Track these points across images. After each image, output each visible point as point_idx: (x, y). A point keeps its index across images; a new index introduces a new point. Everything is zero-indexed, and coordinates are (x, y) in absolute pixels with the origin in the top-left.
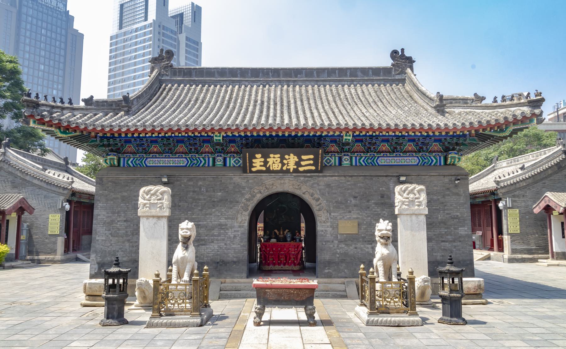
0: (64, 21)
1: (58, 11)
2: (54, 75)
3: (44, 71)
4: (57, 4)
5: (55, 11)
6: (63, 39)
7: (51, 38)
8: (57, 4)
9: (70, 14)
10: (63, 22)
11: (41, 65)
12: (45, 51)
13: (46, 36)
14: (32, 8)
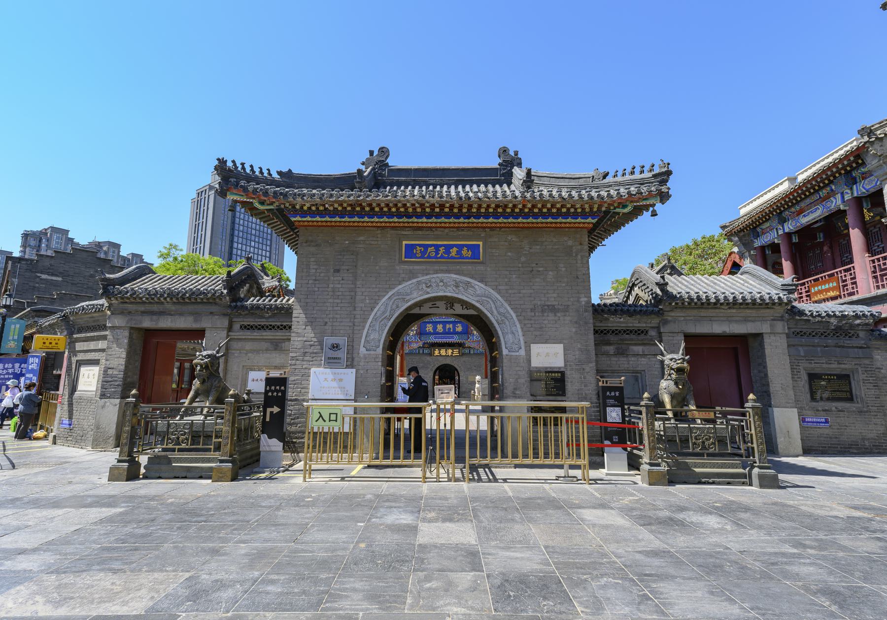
2: (262, 250)
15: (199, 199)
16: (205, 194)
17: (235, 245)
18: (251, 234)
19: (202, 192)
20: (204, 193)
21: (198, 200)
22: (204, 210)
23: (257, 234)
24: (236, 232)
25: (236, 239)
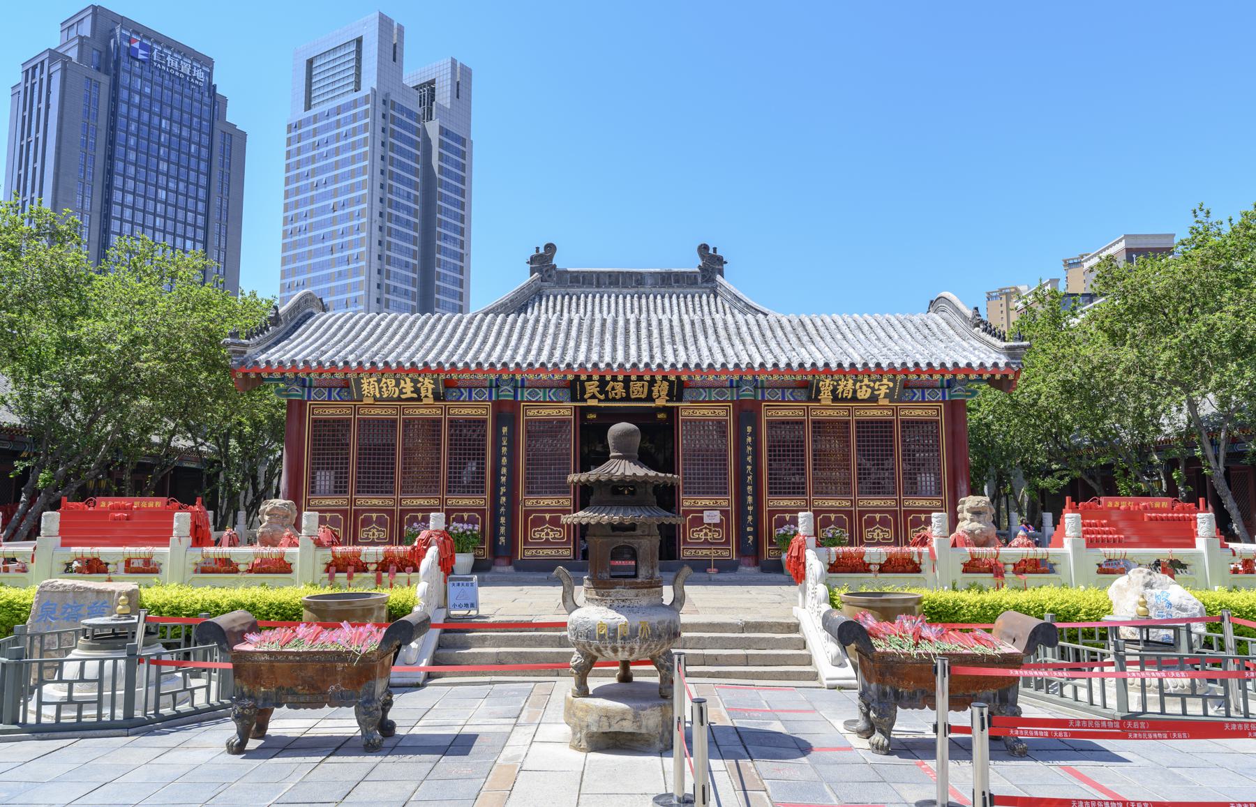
0: (205, 105)
1: (194, 84)
2: (186, 210)
3: (166, 203)
4: (191, 72)
5: (187, 85)
6: (205, 140)
7: (180, 136)
8: (191, 72)
9: (218, 91)
10: (205, 108)
11: (160, 191)
12: (168, 161)
13: (170, 133)
14: (141, 77)
15: (29, 85)
16: (42, 72)
17: (117, 196)
18: (158, 172)
19: (34, 68)
20: (38, 71)
21: (26, 88)
22: (39, 110)
24: (119, 166)
25: (118, 181)
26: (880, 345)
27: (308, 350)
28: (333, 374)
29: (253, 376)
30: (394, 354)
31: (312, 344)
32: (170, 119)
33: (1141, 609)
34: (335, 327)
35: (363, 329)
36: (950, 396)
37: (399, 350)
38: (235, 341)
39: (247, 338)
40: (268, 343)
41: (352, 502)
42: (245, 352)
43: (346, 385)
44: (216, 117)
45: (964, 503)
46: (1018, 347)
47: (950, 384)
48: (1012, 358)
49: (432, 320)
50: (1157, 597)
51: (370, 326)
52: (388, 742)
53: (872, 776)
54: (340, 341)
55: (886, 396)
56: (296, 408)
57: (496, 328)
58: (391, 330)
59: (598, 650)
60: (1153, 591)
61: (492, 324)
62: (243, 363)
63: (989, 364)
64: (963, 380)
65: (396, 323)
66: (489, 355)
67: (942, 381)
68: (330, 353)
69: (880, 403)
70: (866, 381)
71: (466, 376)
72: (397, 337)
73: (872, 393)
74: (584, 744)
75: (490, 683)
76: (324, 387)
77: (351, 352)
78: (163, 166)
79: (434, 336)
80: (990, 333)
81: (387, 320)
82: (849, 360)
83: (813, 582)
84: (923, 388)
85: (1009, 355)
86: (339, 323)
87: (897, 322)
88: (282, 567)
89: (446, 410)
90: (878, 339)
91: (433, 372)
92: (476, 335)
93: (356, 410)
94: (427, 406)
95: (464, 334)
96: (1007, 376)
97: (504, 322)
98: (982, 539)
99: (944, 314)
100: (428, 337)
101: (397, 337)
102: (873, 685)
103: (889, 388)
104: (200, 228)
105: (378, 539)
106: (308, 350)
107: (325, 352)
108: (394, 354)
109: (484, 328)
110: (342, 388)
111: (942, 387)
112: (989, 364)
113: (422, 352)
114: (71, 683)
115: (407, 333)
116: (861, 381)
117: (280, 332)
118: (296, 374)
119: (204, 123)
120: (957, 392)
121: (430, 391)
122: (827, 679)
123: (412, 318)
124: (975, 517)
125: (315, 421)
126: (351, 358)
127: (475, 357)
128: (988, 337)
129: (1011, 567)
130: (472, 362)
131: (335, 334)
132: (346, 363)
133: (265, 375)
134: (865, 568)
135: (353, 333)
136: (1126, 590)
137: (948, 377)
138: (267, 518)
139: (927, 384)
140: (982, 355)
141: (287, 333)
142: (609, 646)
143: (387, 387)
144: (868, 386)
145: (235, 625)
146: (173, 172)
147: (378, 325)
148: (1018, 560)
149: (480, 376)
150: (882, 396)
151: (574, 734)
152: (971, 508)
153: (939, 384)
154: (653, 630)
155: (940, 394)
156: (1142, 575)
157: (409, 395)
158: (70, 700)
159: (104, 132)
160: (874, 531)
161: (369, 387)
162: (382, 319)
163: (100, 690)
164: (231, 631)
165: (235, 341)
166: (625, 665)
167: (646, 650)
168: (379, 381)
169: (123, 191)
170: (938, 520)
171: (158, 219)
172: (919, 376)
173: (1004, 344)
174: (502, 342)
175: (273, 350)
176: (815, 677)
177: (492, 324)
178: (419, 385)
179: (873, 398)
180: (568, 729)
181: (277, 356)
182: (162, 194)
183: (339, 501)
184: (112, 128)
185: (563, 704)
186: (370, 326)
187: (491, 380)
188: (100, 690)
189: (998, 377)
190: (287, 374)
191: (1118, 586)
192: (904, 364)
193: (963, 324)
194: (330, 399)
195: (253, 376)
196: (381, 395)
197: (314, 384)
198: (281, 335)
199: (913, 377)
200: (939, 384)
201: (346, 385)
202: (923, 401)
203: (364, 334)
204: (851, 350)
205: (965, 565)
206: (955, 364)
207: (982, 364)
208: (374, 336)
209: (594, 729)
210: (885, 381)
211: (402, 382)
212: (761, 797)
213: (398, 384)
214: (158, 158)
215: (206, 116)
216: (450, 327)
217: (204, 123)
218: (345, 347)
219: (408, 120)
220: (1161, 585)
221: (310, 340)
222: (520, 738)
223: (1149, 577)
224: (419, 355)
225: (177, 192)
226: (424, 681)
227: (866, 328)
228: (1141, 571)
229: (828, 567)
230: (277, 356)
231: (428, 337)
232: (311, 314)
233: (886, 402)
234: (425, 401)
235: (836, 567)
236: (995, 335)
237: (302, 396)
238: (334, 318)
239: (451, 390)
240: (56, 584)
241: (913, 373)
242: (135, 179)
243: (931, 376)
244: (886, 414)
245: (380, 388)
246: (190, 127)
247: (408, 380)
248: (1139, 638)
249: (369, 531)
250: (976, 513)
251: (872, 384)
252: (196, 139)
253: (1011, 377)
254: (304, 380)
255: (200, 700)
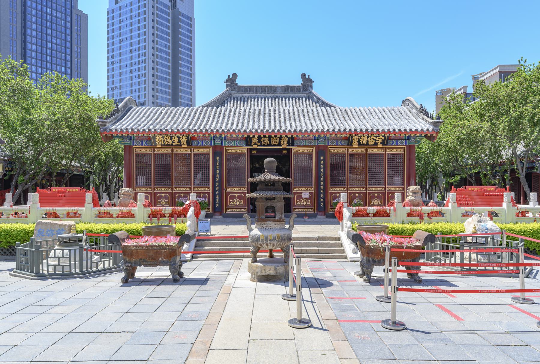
2: (61, 52)
3: (51, 49)
6: (68, 18)
7: (56, 17)
11: (48, 43)
12: (52, 29)
13: (51, 15)
17: (29, 46)
18: (47, 34)
23: (54, 34)
24: (29, 31)
25: (28, 39)
26: (379, 121)
27: (132, 124)
28: (144, 135)
29: (110, 135)
30: (170, 126)
31: (133, 121)
32: (51, 8)
33: (474, 230)
34: (143, 113)
35: (155, 114)
36: (409, 143)
37: (171, 124)
38: (101, 120)
39: (106, 119)
40: (115, 121)
41: (153, 189)
42: (106, 125)
43: (149, 139)
44: (73, 7)
45: (410, 188)
46: (438, 122)
47: (409, 138)
48: (435, 127)
49: (185, 110)
50: (482, 226)
51: (158, 113)
52: (181, 279)
53: (362, 289)
54: (145, 120)
55: (381, 143)
56: (128, 149)
57: (213, 114)
58: (167, 115)
59: (261, 245)
60: (481, 223)
61: (211, 112)
62: (105, 130)
63: (425, 129)
64: (414, 136)
65: (169, 112)
66: (211, 126)
67: (405, 136)
68: (142, 125)
69: (378, 146)
70: (373, 137)
71: (201, 135)
72: (170, 118)
73: (375, 142)
74: (256, 279)
75: (217, 260)
76: (140, 140)
77: (151, 125)
78: (49, 31)
79: (186, 118)
80: (426, 116)
81: (165, 110)
82: (365, 128)
83: (346, 221)
84: (397, 140)
85: (434, 125)
86: (144, 111)
87: (387, 111)
88: (131, 215)
89: (192, 150)
90: (379, 118)
91: (187, 134)
92: (204, 117)
93: (154, 150)
94: (184, 148)
95: (199, 116)
96: (433, 134)
97: (216, 111)
98: (416, 203)
99: (408, 107)
100: (183, 118)
101: (170, 118)
102: (365, 258)
103: (382, 140)
104: (68, 61)
105: (165, 204)
106: (132, 124)
107: (140, 125)
108: (170, 126)
109: (208, 114)
110: (147, 140)
111: (405, 139)
112: (425, 129)
113: (182, 125)
114: (59, 258)
115: (174, 116)
116: (371, 137)
117: (119, 116)
118: (128, 135)
119: (67, 10)
120: (412, 142)
121: (185, 142)
122: (350, 258)
123: (176, 109)
124: (414, 195)
125: (136, 154)
126: (151, 127)
127: (205, 127)
128: (426, 118)
129: (427, 215)
130: (203, 129)
131: (143, 117)
132: (149, 130)
133: (114, 135)
134: (368, 215)
135: (151, 116)
136: (471, 223)
137: (407, 135)
138: (122, 196)
139: (399, 138)
140: (423, 126)
141: (122, 116)
142: (265, 243)
143: (167, 140)
144: (373, 139)
145: (122, 236)
146: (54, 34)
147: (161, 112)
148: (429, 212)
149: (207, 135)
150: (379, 143)
151: (252, 276)
152: (412, 191)
153: (404, 138)
154: (282, 237)
155: (404, 142)
156: (477, 217)
157: (176, 143)
158: (59, 265)
159: (20, 15)
160: (374, 201)
161: (159, 140)
162: (163, 110)
163: (70, 262)
164: (121, 239)
165: (101, 120)
166: (271, 251)
167: (279, 245)
168: (163, 138)
169: (31, 43)
170: (398, 196)
171: (48, 57)
172: (395, 135)
173: (432, 121)
174: (216, 120)
175: (117, 124)
176: (346, 257)
177: (211, 112)
178: (180, 139)
179: (376, 144)
180: (250, 275)
181: (119, 127)
182: (49, 45)
183: (149, 189)
184: (24, 13)
185: (247, 265)
186: (158, 113)
187: (211, 137)
188: (70, 262)
189: (429, 135)
190: (124, 135)
191: (468, 222)
192: (389, 130)
193: (416, 111)
194: (142, 145)
195: (110, 135)
196: (164, 144)
197: (135, 139)
198: (120, 117)
199: (392, 135)
200: (404, 138)
201: (149, 139)
202: (397, 145)
203: (156, 116)
204: (366, 123)
205: (408, 214)
206: (411, 130)
207: (422, 129)
208: (160, 118)
209: (259, 274)
210: (381, 137)
211: (173, 137)
212: (321, 295)
213: (171, 139)
214: (47, 27)
215: (68, 6)
216: (193, 113)
217: (67, 10)
218: (148, 122)
219: (164, 9)
220: (484, 221)
221: (133, 119)
222: (231, 279)
223: (480, 218)
224: (180, 126)
225: (56, 44)
226: (191, 259)
227: (373, 113)
228: (477, 216)
229: (352, 215)
230: (119, 127)
231: (183, 118)
232: (132, 108)
233: (381, 146)
234: (183, 146)
235: (355, 215)
236: (428, 117)
237: (130, 144)
238: (142, 109)
239: (194, 141)
240: (43, 222)
241: (393, 133)
242: (36, 38)
243: (400, 135)
244: (381, 151)
245: (164, 141)
246: (61, 12)
247: (176, 137)
248: (471, 241)
249: (161, 201)
250: (414, 193)
251: (375, 138)
252: (64, 18)
253: (434, 135)
254: (131, 137)
255: (107, 265)
